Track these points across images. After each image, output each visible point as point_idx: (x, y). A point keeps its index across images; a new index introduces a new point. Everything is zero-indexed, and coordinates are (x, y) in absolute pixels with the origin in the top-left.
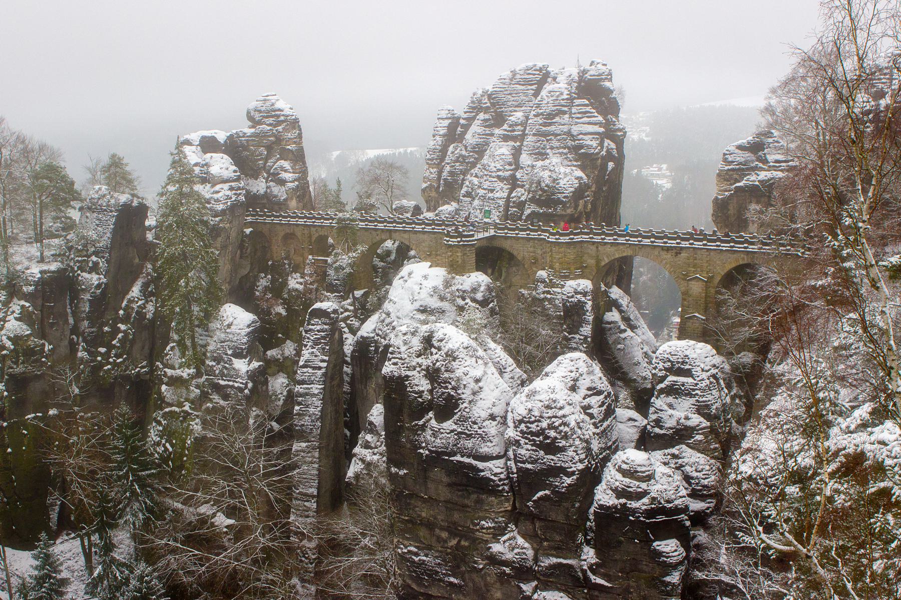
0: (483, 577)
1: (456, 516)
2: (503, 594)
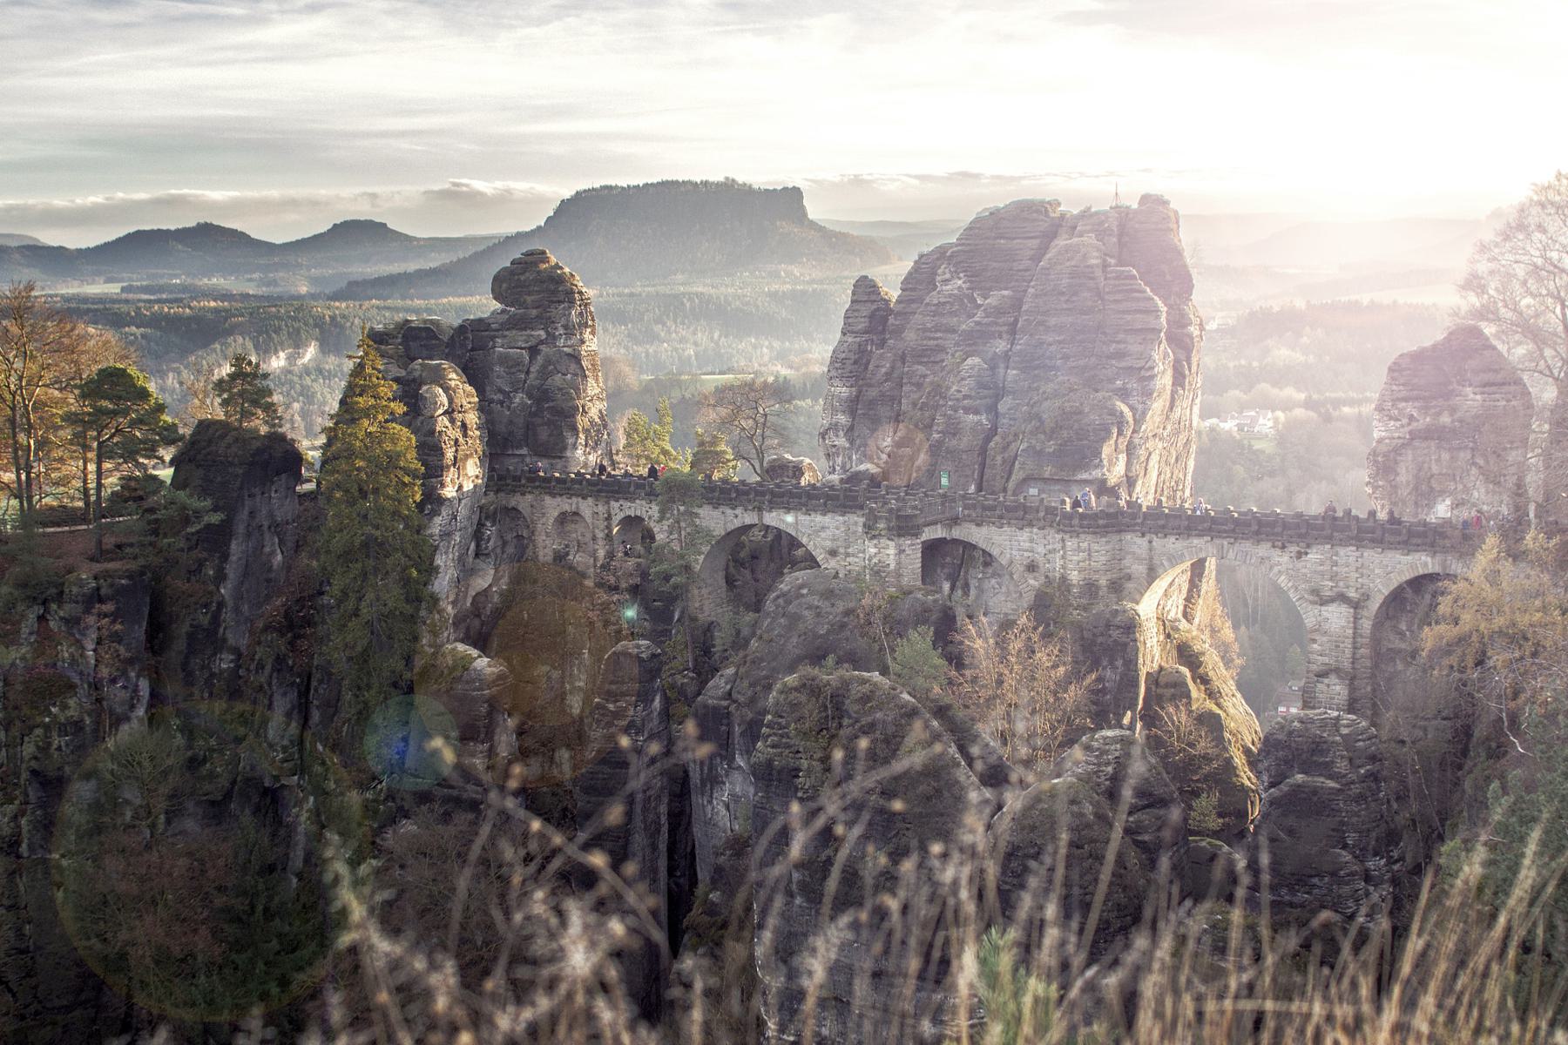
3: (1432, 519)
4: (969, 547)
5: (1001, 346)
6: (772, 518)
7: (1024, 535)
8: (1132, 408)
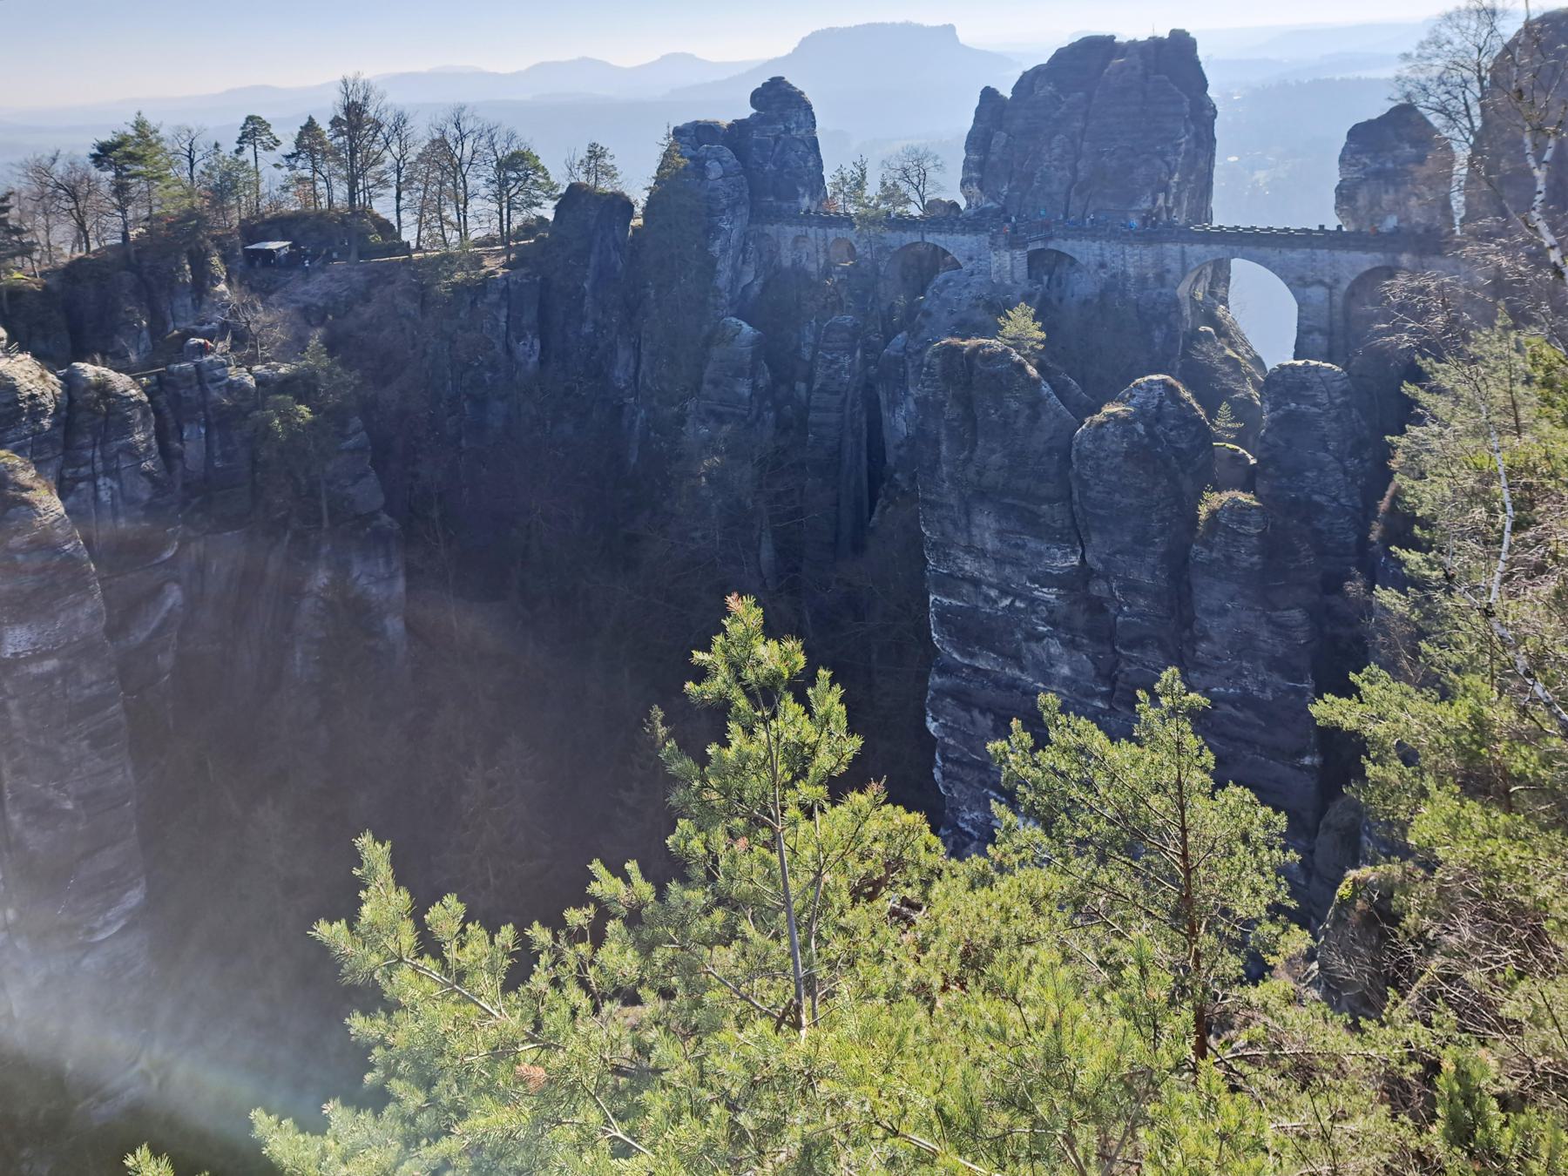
0: (1046, 649)
1: (1008, 570)
2: (1072, 669)
3: (1383, 229)
4: (1060, 255)
5: (1078, 125)
6: (929, 238)
7: (1096, 246)
8: (1168, 164)
